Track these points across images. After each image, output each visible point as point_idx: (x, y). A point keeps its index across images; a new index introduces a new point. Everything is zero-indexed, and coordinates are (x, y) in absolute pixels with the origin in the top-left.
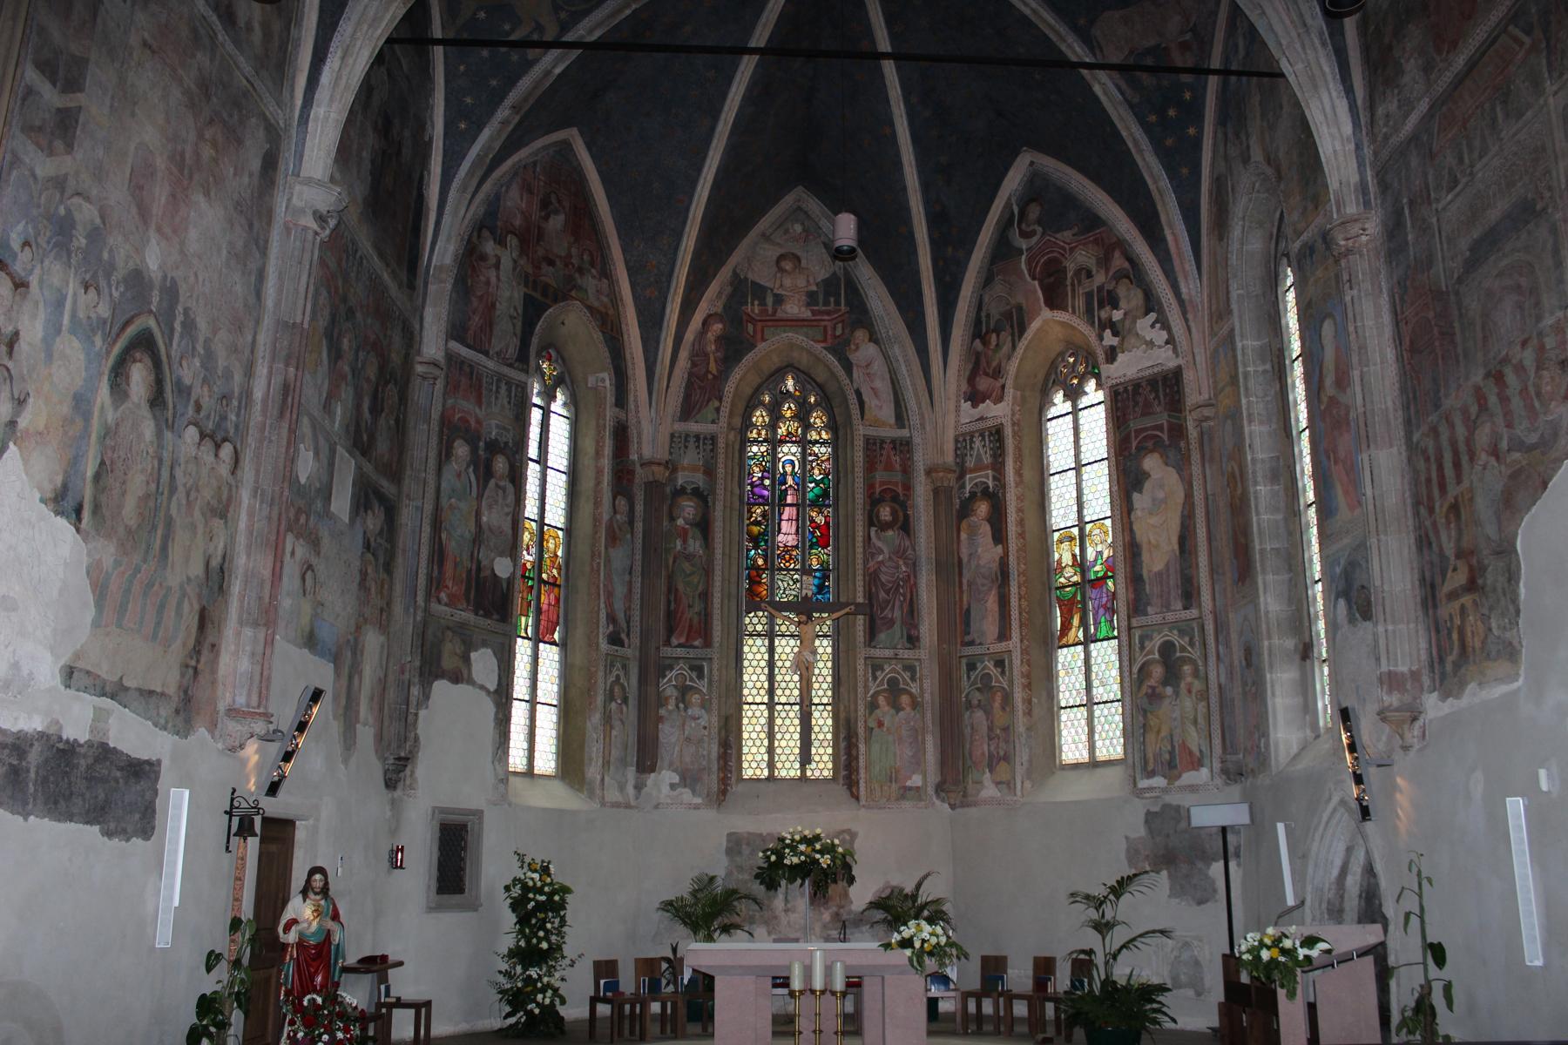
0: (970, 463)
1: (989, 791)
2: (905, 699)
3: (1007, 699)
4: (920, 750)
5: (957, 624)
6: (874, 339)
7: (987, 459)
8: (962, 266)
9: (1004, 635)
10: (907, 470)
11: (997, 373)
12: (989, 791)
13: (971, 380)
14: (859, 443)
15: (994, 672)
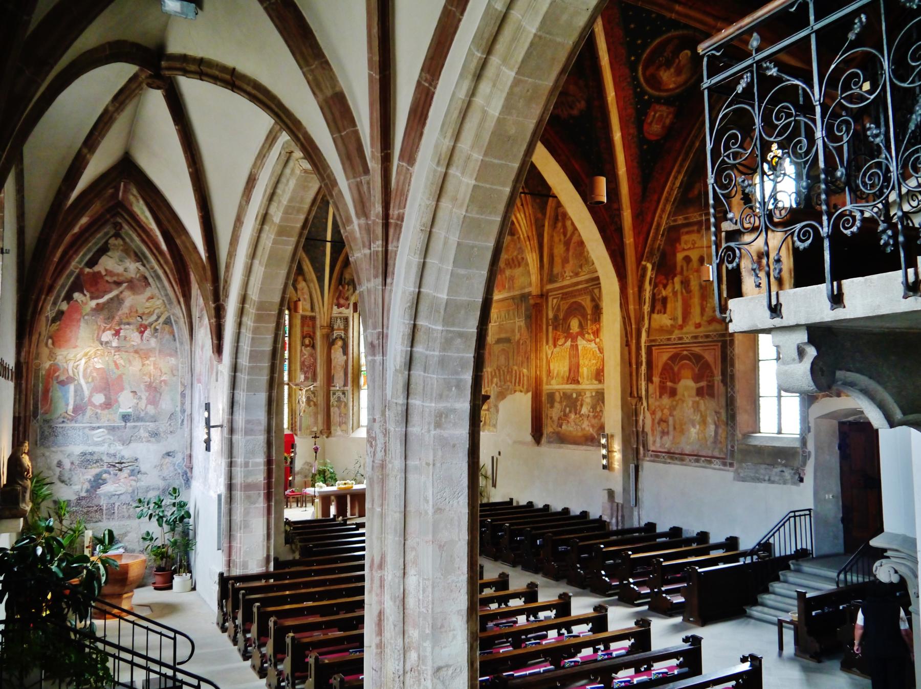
0: (336, 327)
1: (339, 432)
2: (312, 403)
3: (346, 405)
4: (316, 419)
5: (330, 379)
6: (305, 280)
7: (342, 327)
8: (337, 260)
9: (345, 385)
10: (314, 327)
11: (347, 299)
12: (339, 432)
13: (338, 299)
14: (299, 317)
15: (342, 396)
